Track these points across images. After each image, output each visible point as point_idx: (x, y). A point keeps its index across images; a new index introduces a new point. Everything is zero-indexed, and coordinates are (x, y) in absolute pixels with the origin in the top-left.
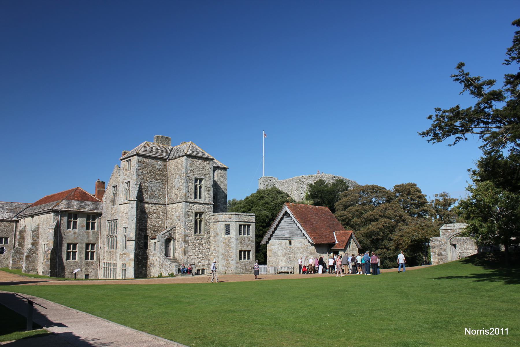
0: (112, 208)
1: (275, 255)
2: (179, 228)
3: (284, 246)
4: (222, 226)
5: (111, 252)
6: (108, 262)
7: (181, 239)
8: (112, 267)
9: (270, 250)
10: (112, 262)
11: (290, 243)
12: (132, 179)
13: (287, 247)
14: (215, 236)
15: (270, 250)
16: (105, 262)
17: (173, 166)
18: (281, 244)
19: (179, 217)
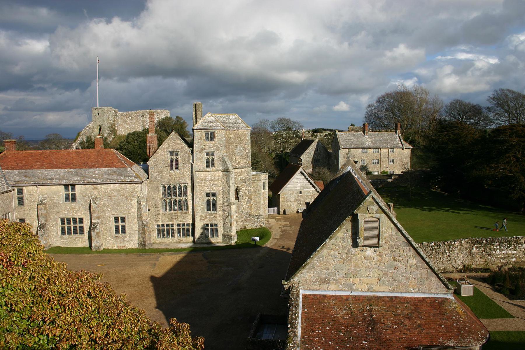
0: (169, 172)
1: (287, 201)
2: (243, 189)
3: (295, 195)
4: (262, 184)
5: (172, 214)
6: (165, 223)
7: (247, 198)
8: (176, 228)
9: (284, 198)
10: (175, 223)
11: (301, 193)
12: (218, 150)
13: (298, 196)
14: (254, 192)
15: (284, 198)
16: (160, 223)
17: (232, 137)
18: (293, 193)
19: (245, 180)
